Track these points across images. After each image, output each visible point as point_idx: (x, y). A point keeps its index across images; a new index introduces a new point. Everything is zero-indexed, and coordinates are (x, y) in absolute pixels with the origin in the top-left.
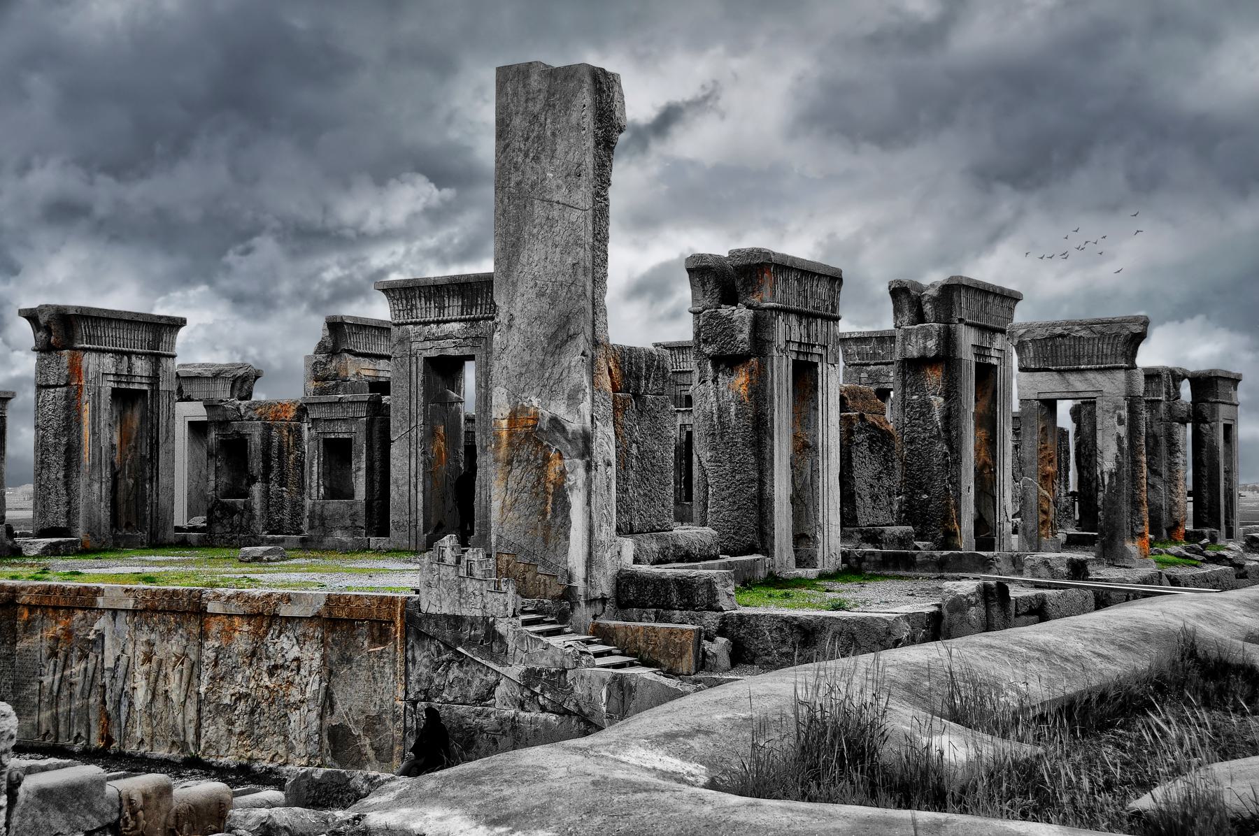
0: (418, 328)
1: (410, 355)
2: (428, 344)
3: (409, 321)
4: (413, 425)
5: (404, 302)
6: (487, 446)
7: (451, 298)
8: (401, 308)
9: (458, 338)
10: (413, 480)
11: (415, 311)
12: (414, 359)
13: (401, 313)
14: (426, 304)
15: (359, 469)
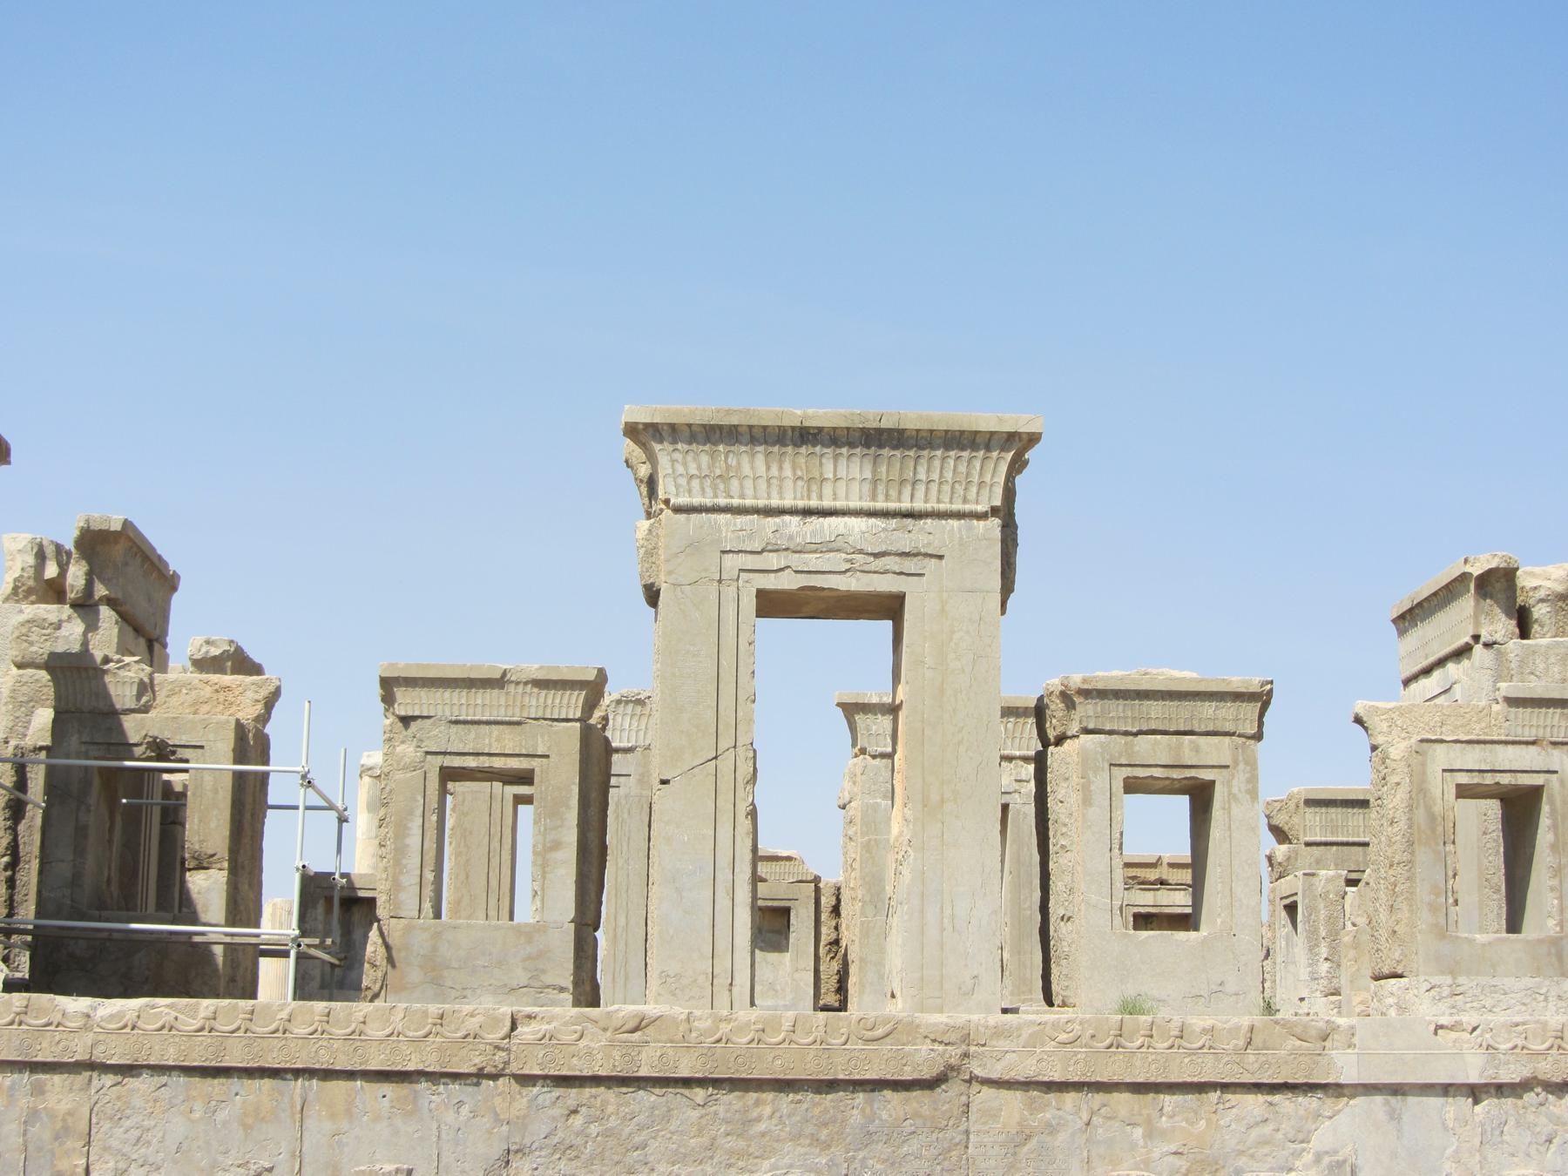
0: (741, 520)
1: (720, 581)
2: (773, 561)
3: (722, 501)
4: (723, 745)
5: (705, 459)
6: (942, 801)
7: (843, 462)
8: (693, 470)
9: (861, 552)
10: (724, 876)
11: (735, 483)
12: (733, 589)
13: (695, 483)
14: (768, 468)
15: (556, 845)
